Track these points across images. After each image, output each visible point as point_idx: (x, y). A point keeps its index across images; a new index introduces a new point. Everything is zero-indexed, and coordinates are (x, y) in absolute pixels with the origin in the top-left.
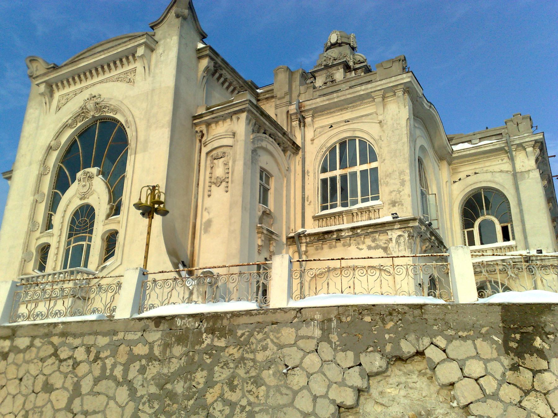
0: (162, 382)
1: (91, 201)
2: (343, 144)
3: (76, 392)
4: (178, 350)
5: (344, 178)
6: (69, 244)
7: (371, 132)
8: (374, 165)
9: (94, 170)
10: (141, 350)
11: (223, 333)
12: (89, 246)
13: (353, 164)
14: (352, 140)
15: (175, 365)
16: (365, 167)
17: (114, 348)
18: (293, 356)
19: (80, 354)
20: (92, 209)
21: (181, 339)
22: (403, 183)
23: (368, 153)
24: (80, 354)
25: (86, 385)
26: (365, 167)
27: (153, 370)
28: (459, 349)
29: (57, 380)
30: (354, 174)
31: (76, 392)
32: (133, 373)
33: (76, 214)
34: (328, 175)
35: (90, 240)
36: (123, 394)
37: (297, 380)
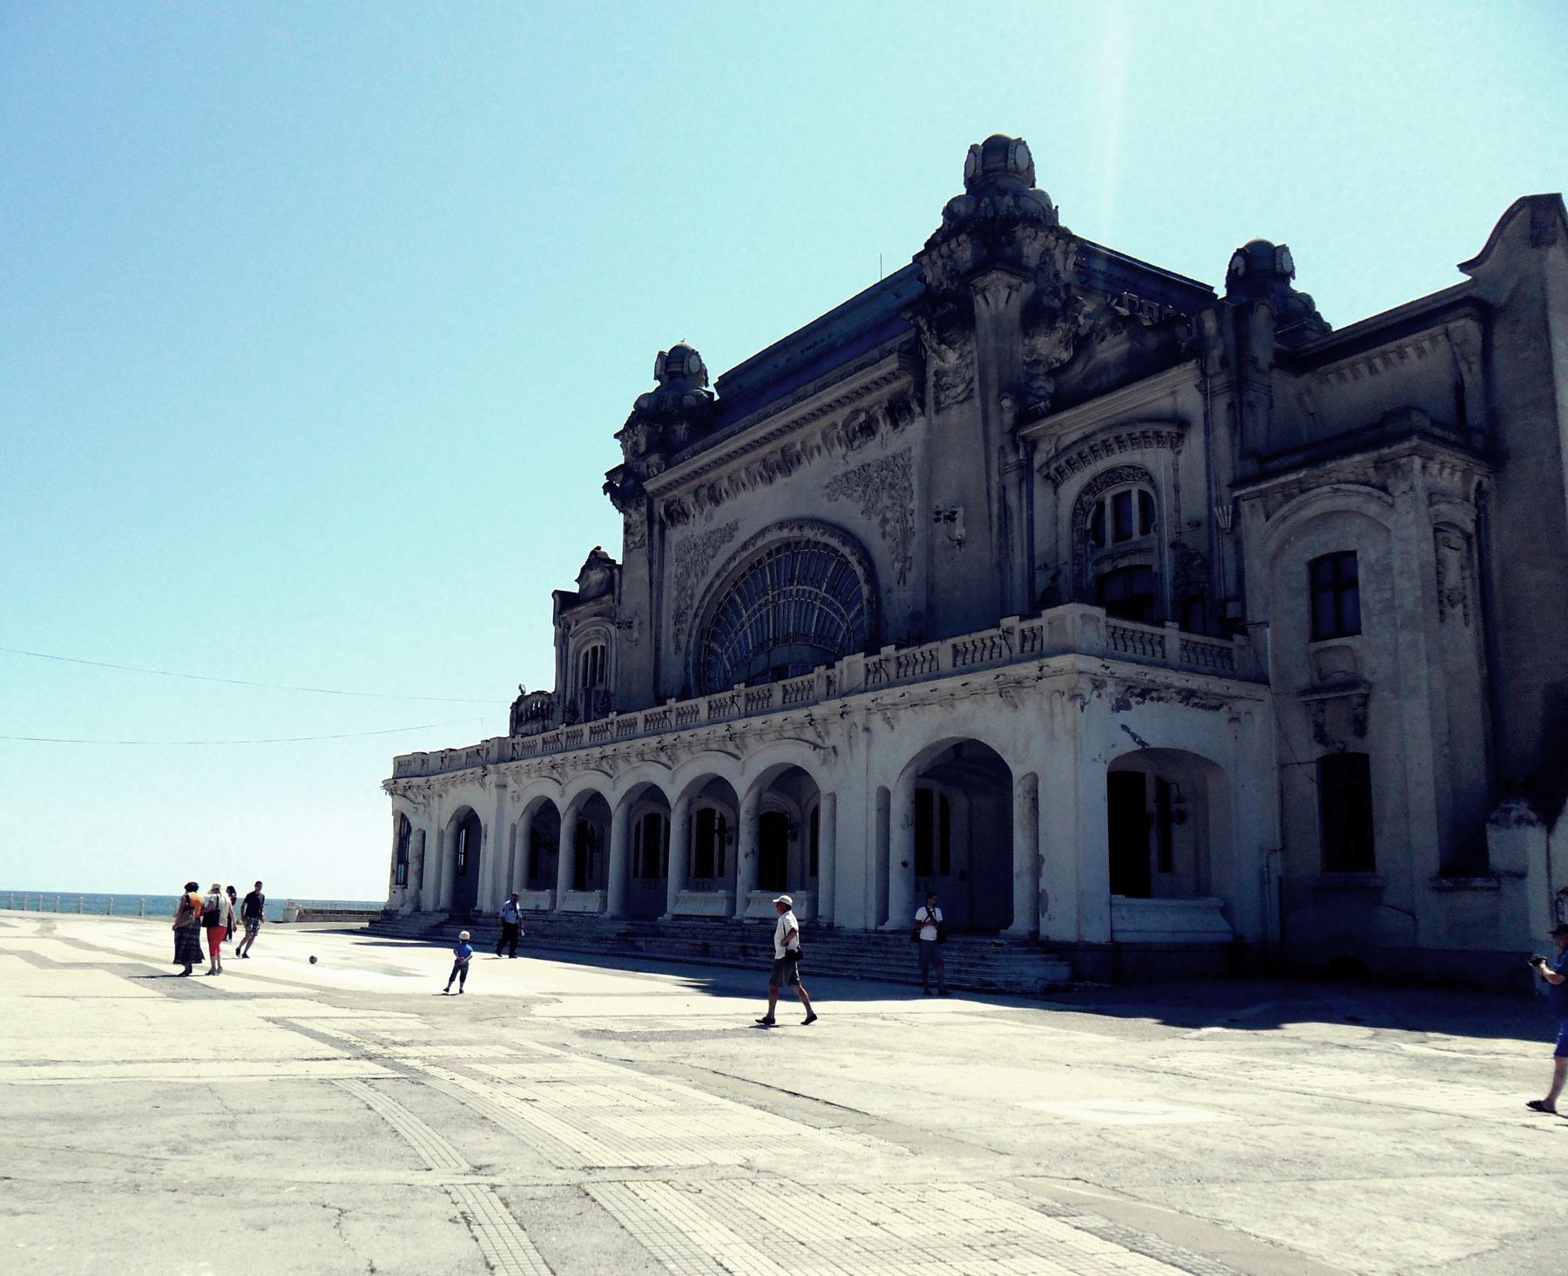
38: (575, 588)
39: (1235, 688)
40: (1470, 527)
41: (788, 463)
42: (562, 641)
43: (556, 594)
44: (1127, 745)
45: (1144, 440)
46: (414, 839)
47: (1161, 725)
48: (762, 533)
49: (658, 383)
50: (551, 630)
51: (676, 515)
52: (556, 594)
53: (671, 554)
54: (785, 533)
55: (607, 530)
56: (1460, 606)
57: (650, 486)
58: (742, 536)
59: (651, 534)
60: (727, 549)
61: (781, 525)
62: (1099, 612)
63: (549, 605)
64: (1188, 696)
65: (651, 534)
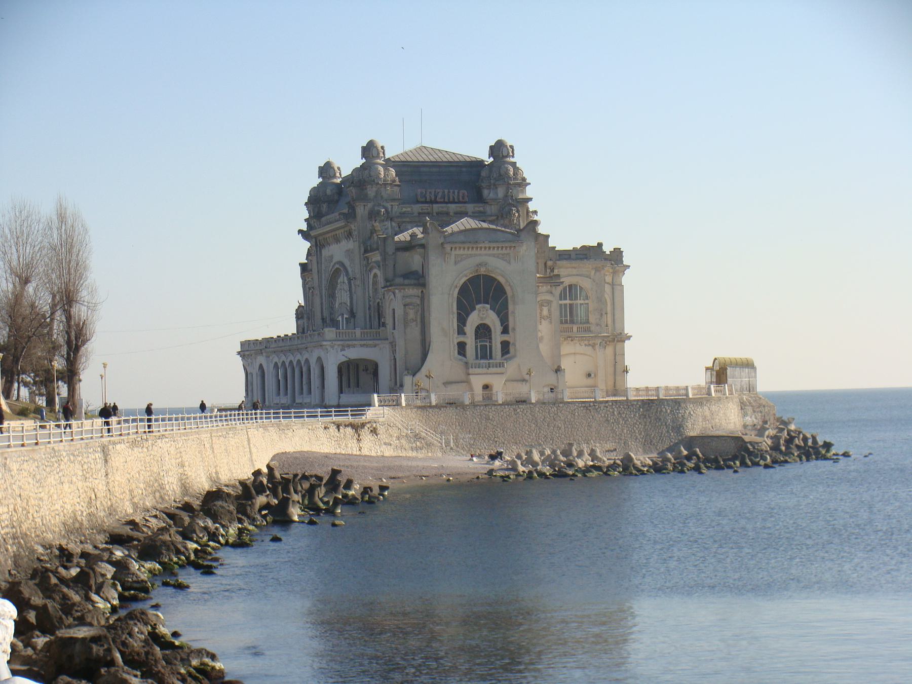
1: (487, 322)
2: (570, 286)
5: (571, 305)
6: (476, 343)
9: (488, 306)
12: (491, 347)
13: (576, 299)
14: (576, 286)
16: (582, 302)
30: (577, 304)
35: (490, 342)
39: (377, 342)
40: (419, 302)
41: (337, 240)
43: (300, 264)
44: (344, 359)
47: (354, 353)
49: (321, 180)
50: (300, 281)
52: (300, 264)
54: (337, 266)
55: (308, 245)
57: (313, 233)
60: (332, 264)
62: (334, 329)
63: (299, 268)
64: (362, 346)
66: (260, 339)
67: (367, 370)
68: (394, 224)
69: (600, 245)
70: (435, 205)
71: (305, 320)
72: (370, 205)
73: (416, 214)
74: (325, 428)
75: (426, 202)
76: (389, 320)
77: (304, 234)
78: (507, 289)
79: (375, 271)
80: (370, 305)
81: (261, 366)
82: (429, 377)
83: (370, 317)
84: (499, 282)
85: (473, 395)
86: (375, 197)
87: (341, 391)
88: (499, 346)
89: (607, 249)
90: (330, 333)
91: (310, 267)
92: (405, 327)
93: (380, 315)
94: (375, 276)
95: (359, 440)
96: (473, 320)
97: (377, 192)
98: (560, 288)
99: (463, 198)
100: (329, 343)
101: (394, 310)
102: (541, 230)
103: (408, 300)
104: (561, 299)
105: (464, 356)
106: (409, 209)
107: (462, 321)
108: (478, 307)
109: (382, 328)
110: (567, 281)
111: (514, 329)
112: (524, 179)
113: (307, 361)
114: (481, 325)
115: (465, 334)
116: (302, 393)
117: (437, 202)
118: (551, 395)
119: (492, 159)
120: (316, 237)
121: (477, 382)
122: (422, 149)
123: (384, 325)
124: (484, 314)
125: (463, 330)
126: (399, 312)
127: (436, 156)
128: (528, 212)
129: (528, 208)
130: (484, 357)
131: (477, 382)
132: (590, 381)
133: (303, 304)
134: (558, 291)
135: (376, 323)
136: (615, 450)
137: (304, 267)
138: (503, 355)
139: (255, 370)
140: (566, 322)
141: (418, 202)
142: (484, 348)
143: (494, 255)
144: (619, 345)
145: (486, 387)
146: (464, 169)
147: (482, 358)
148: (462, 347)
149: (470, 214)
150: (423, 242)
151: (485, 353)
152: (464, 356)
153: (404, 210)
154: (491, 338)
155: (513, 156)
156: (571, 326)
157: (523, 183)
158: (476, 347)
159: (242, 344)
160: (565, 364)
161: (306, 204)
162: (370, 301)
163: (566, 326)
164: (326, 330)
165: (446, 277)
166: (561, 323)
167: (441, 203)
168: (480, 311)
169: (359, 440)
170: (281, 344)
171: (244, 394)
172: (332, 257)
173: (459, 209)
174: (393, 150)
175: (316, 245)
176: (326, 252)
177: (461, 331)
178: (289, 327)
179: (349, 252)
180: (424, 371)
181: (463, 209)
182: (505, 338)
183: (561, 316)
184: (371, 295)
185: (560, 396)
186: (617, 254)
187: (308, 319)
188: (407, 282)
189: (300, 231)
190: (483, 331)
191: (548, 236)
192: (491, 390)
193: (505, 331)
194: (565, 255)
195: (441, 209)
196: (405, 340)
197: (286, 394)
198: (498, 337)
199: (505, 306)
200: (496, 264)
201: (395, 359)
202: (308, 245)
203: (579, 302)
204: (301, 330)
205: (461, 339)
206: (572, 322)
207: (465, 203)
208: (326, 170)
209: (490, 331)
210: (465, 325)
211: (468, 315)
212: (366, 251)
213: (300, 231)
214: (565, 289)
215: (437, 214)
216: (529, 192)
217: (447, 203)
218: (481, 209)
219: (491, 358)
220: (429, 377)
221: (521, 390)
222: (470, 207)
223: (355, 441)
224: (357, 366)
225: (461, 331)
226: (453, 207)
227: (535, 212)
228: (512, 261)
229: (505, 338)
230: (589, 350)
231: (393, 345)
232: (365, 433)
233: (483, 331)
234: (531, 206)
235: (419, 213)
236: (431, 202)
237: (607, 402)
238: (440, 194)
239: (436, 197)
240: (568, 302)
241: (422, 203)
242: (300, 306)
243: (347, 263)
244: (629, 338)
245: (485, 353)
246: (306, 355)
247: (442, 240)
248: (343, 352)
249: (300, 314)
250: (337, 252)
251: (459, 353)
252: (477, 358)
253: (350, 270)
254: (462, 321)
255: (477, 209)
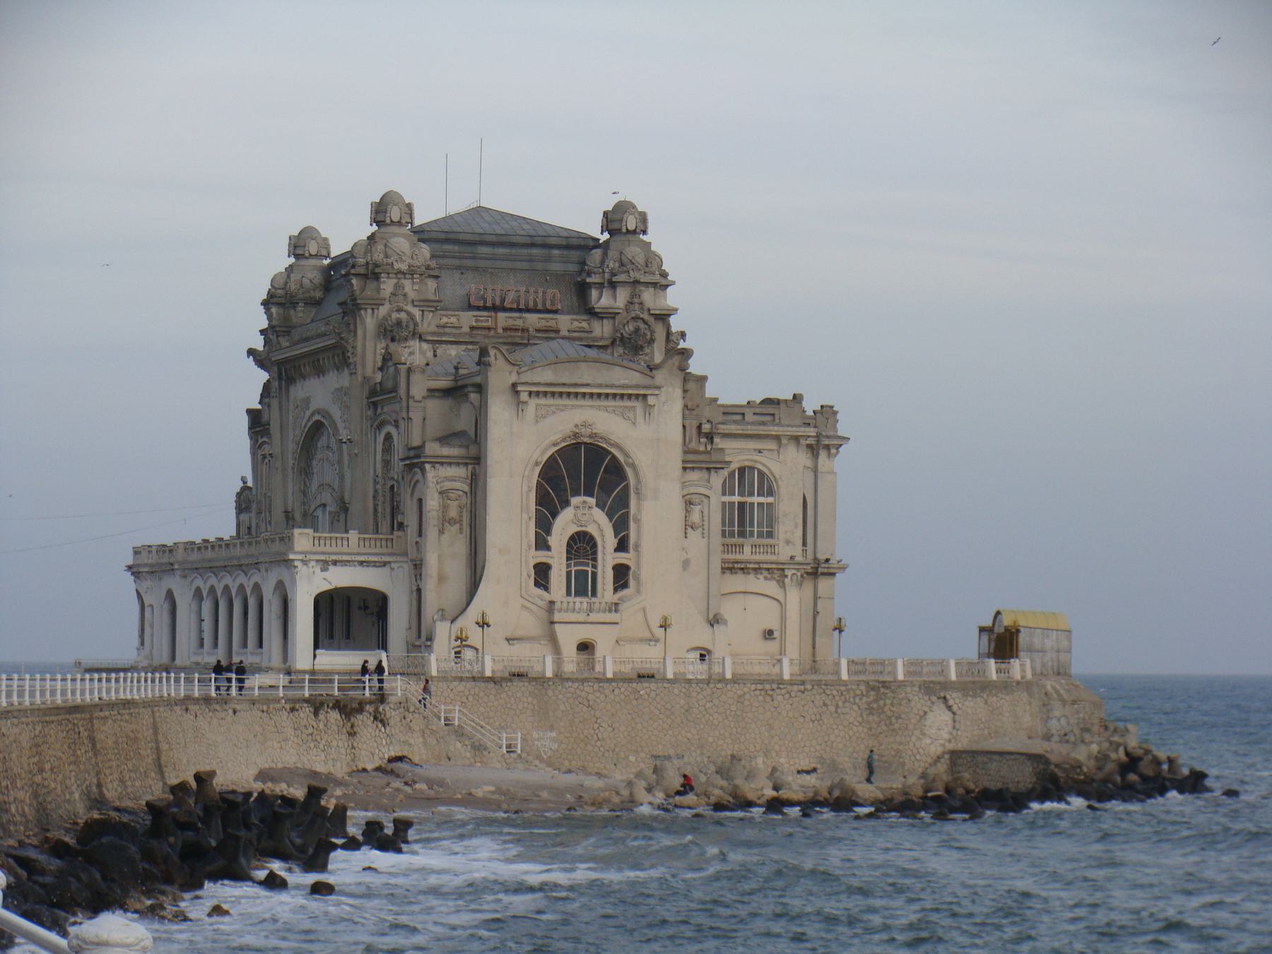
0: (868, 704)
1: (591, 529)
2: (742, 470)
3: (837, 706)
4: (872, 693)
5: (742, 505)
6: (568, 566)
7: (773, 469)
8: (770, 500)
9: (592, 501)
10: (858, 692)
11: (888, 688)
12: (594, 575)
13: (751, 494)
14: (752, 468)
15: (871, 698)
16: (762, 500)
17: (848, 691)
18: (910, 697)
19: (835, 692)
20: (592, 538)
21: (873, 689)
22: (796, 526)
23: (767, 486)
24: (835, 692)
25: (840, 704)
26: (762, 500)
27: (865, 699)
28: (954, 695)
29: (828, 702)
30: (752, 504)
31: (837, 706)
32: (857, 700)
33: (572, 538)
34: (727, 499)
35: (595, 567)
36: (856, 708)
37: (913, 704)
38: (259, 407)
40: (466, 488)
41: (320, 371)
42: (254, 454)
43: (249, 412)
44: (326, 587)
45: (389, 423)
46: (148, 611)
48: (313, 414)
49: (292, 260)
50: (246, 442)
51: (290, 380)
52: (249, 412)
53: (291, 407)
54: (317, 417)
55: (264, 376)
56: (458, 525)
58: (313, 407)
59: (280, 388)
60: (308, 413)
61: (318, 412)
62: (310, 531)
63: (245, 421)
65: (280, 388)
66: (170, 544)
67: (366, 608)
68: (425, 345)
69: (797, 398)
70: (501, 315)
71: (253, 514)
72: (383, 311)
73: (466, 329)
74: (292, 710)
75: (485, 308)
76: (411, 520)
77: (260, 359)
78: (629, 472)
79: (390, 428)
80: (376, 491)
81: (170, 596)
82: (483, 624)
83: (375, 510)
84: (614, 457)
85: (558, 662)
86: (393, 294)
87: (316, 646)
88: (610, 574)
89: (810, 406)
90: (303, 539)
91: (265, 417)
92: (442, 532)
93: (395, 510)
94: (388, 437)
95: (352, 734)
96: (564, 526)
97: (397, 286)
98: (725, 473)
99: (553, 304)
100: (300, 557)
101: (420, 501)
102: (695, 367)
103: (448, 485)
104: (724, 494)
105: (546, 589)
106: (453, 320)
107: (544, 525)
108: (575, 501)
109: (400, 533)
110: (737, 462)
111: (637, 546)
112: (664, 275)
113: (257, 587)
114: (578, 533)
115: (548, 548)
116: (245, 645)
117: (505, 309)
118: (703, 667)
119: (606, 236)
120: (280, 363)
121: (569, 637)
122: (479, 212)
123: (401, 526)
124: (582, 514)
125: (546, 542)
126: (433, 503)
127: (506, 226)
128: (669, 334)
129: (668, 327)
130: (581, 592)
131: (569, 637)
132: (773, 646)
133: (250, 484)
134: (717, 480)
135: (385, 525)
136: (814, 770)
137: (255, 417)
138: (616, 590)
139: (155, 598)
140: (732, 534)
141: (470, 307)
142: (582, 575)
143: (606, 409)
144: (823, 583)
145: (585, 647)
146: (556, 252)
147: (578, 594)
148: (542, 574)
149: (564, 333)
150: (478, 380)
151: (582, 586)
152: (546, 589)
153: (445, 320)
154: (595, 560)
155: (644, 232)
156: (741, 540)
157: (662, 285)
158: (569, 574)
159: (137, 552)
160: (729, 609)
161: (266, 304)
162: (376, 482)
163: (729, 541)
164: (297, 531)
165: (519, 442)
166: (724, 535)
167: (511, 310)
168: (577, 507)
169: (352, 734)
170: (209, 554)
171: (136, 641)
172: (307, 401)
173: (543, 324)
174: (428, 211)
175: (280, 378)
176: (299, 391)
177: (542, 544)
178: (223, 524)
179: (341, 394)
180: (473, 613)
181: (552, 324)
182: (622, 558)
183: (724, 524)
184: (379, 472)
185: (717, 669)
186: (827, 413)
187: (259, 513)
188: (446, 451)
189: (251, 352)
190: (582, 545)
191: (702, 379)
192: (593, 653)
193: (622, 546)
194: (731, 412)
195: (510, 323)
196: (443, 554)
197: (216, 645)
198: (608, 557)
199: (623, 501)
200: (607, 424)
201: (419, 591)
202: (264, 376)
203: (756, 499)
204: (245, 532)
205: (542, 556)
206: (742, 534)
207: (556, 312)
208: (298, 246)
209: (595, 545)
210: (548, 532)
211: (554, 515)
212: (373, 393)
213: (251, 352)
214: (732, 474)
215: (505, 329)
216: (672, 297)
217: (520, 310)
218: (584, 324)
219: (594, 594)
220: (483, 624)
221: (647, 656)
222: (565, 322)
223: (345, 737)
224: (349, 598)
225: (542, 544)
226: (533, 320)
227: (683, 335)
228: (640, 419)
229: (622, 558)
230: (771, 587)
231: (418, 567)
232: (364, 721)
233: (582, 545)
234: (676, 324)
235: (472, 328)
236: (495, 308)
237: (803, 683)
238: (511, 296)
239: (503, 300)
240: (736, 499)
241: (479, 308)
242: (245, 488)
243: (336, 413)
244: (844, 568)
245: (582, 586)
246: (256, 578)
247: (514, 378)
248: (325, 574)
249: (244, 501)
250: (318, 392)
251: (537, 584)
252: (568, 593)
253: (340, 425)
254: (544, 525)
255: (576, 324)
